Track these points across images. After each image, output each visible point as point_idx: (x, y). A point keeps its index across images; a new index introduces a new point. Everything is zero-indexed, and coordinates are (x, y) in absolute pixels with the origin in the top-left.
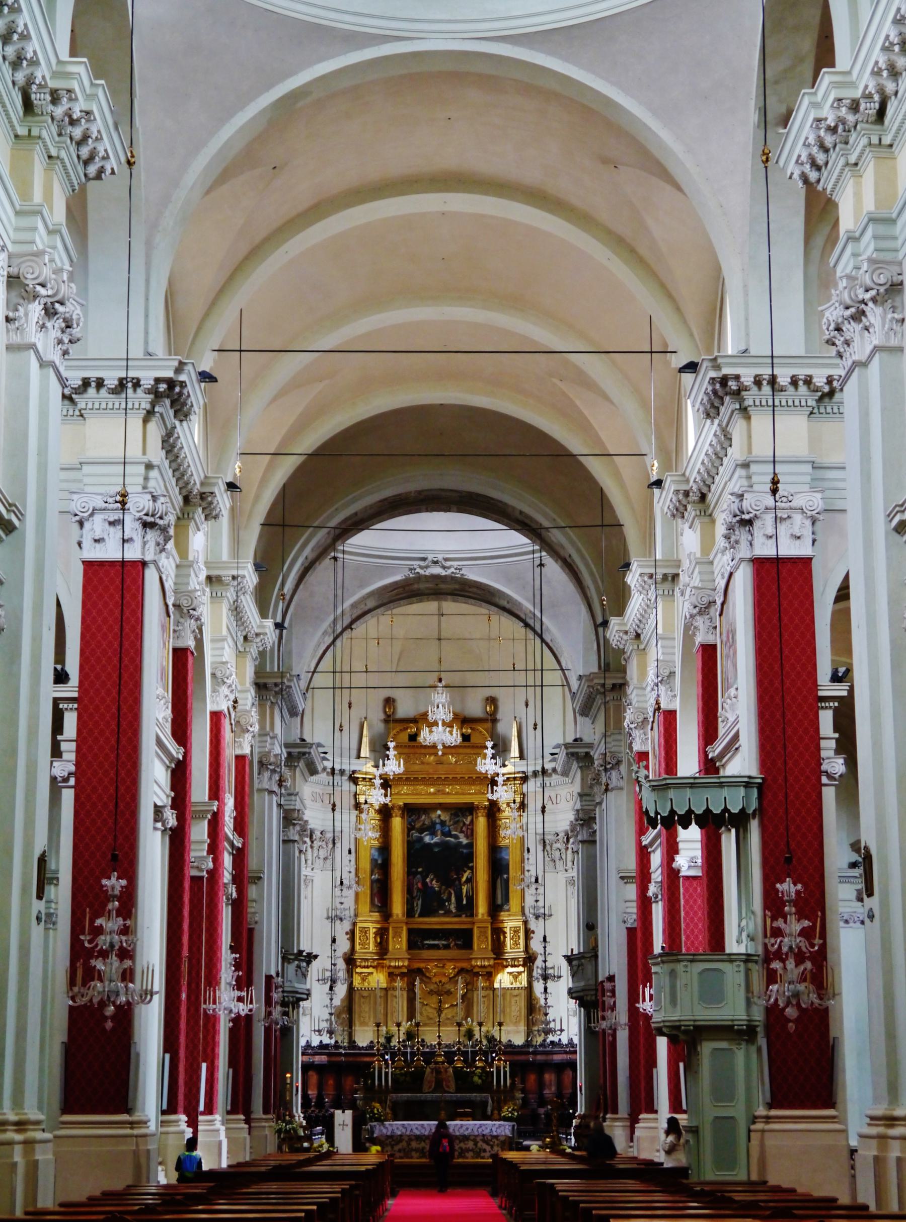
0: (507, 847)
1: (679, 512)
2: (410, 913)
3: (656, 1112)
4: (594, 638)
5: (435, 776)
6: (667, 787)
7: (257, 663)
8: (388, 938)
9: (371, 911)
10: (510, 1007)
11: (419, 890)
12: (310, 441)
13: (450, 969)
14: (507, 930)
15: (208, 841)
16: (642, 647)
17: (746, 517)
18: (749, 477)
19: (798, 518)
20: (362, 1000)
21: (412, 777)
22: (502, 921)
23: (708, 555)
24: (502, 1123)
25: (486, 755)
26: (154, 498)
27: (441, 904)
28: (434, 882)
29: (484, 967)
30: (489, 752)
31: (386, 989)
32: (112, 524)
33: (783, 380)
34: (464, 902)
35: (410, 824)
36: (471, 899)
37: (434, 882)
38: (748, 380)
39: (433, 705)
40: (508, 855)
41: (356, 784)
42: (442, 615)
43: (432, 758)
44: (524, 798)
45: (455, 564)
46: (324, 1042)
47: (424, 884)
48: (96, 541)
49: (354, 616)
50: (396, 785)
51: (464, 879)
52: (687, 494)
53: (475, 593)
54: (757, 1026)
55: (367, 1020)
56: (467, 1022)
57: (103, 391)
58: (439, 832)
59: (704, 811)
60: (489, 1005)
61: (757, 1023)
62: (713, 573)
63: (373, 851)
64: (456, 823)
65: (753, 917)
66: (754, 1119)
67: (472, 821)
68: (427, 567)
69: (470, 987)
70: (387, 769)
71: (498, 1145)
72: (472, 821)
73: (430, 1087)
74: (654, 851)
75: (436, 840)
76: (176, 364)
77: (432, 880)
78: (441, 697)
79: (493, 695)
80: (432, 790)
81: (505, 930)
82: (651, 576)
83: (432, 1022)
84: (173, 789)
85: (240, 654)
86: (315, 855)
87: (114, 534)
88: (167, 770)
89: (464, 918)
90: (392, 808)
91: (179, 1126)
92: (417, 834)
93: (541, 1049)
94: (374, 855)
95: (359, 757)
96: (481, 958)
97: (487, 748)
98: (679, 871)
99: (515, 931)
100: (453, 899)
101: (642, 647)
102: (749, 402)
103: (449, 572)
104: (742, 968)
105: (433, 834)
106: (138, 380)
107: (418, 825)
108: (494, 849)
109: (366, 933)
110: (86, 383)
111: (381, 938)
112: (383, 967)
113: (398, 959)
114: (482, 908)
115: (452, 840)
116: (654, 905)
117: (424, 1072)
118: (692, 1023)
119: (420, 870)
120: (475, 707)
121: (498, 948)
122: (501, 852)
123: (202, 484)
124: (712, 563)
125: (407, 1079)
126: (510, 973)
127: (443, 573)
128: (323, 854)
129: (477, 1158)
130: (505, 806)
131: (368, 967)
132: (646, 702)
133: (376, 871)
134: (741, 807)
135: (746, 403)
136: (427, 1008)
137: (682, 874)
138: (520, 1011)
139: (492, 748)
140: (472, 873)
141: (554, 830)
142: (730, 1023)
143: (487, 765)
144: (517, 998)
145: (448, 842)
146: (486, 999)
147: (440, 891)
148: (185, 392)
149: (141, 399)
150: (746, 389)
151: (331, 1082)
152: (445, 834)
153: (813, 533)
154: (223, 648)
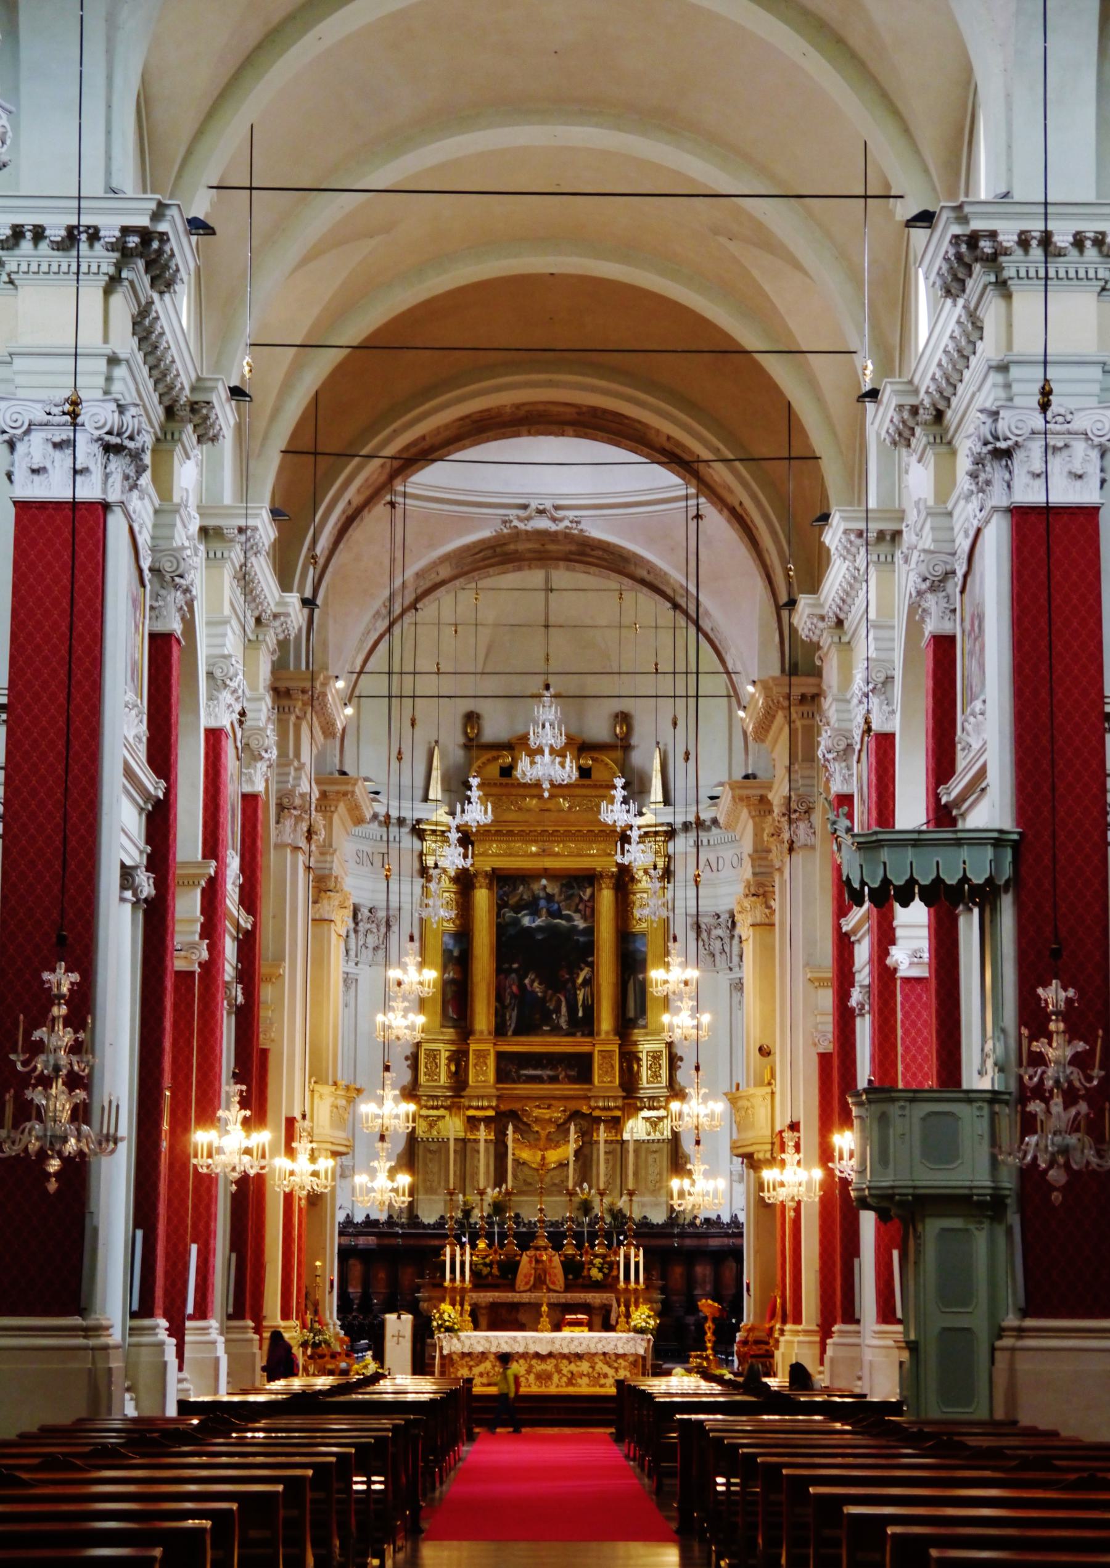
1: (903, 437)
2: (500, 1031)
3: (858, 1322)
4: (776, 626)
5: (539, 829)
6: (878, 845)
7: (275, 658)
8: (467, 1065)
9: (443, 1026)
10: (646, 1168)
11: (513, 996)
12: (355, 331)
14: (643, 1056)
15: (202, 919)
16: (845, 639)
17: (1002, 445)
18: (1008, 386)
19: (1079, 447)
20: (429, 1156)
21: (505, 829)
22: (635, 1043)
23: (945, 502)
24: (632, 1334)
25: (613, 797)
26: (121, 409)
27: (546, 1017)
28: (536, 984)
29: (609, 1109)
30: (619, 794)
32: (58, 446)
33: (1063, 239)
34: (580, 1014)
35: (500, 898)
36: (590, 1010)
37: (536, 984)
38: (1008, 239)
39: (536, 723)
40: (645, 945)
41: (422, 838)
42: (551, 590)
43: (534, 801)
44: (669, 862)
45: (571, 514)
46: (373, 1217)
47: (522, 987)
48: (35, 471)
49: (419, 591)
50: (480, 841)
51: (580, 980)
52: (914, 411)
53: (598, 558)
54: (1007, 1196)
55: (435, 1184)
56: (582, 1189)
57: (44, 246)
58: (544, 911)
59: (933, 880)
61: (1007, 1192)
62: (952, 529)
63: (446, 939)
64: (569, 898)
65: (1002, 1037)
66: (1000, 1332)
67: (592, 896)
68: (529, 518)
69: (586, 1139)
70: (467, 817)
71: (625, 1368)
72: (592, 896)
73: (527, 1283)
74: (859, 941)
75: (539, 922)
76: (153, 205)
77: (532, 982)
78: (548, 712)
79: (626, 710)
80: (534, 849)
81: (640, 1055)
82: (860, 534)
83: (531, 1188)
84: (148, 841)
85: (251, 645)
86: (361, 943)
87: (61, 462)
88: (140, 814)
90: (475, 875)
91: (156, 1334)
92: (512, 914)
93: (691, 1230)
94: (446, 944)
95: (426, 799)
97: (615, 787)
98: (895, 970)
99: (653, 1057)
100: (564, 1010)
101: (845, 639)
102: (1009, 272)
103: (561, 526)
104: (986, 1112)
105: (535, 913)
106: (97, 229)
108: (625, 936)
109: (435, 1057)
110: (18, 233)
111: (457, 1066)
112: (459, 1108)
114: (606, 1022)
115: (563, 922)
116: (858, 1020)
117: (519, 1262)
118: (910, 1191)
119: (515, 966)
120: (599, 729)
121: (629, 1083)
122: (634, 942)
123: (193, 389)
124: (950, 514)
125: (495, 1271)
126: (647, 1119)
127: (553, 527)
128: (372, 940)
129: (593, 1386)
130: (641, 873)
131: (437, 1108)
132: (851, 720)
133: (450, 967)
134: (987, 875)
135: (1006, 274)
136: (525, 1169)
137: (899, 974)
139: (623, 788)
140: (593, 972)
141: (712, 909)
142: (966, 1191)
143: (615, 814)
144: (655, 1156)
145: (556, 926)
146: (610, 1157)
147: (544, 998)
148: (167, 248)
149: (102, 260)
150: (1006, 252)
151: (382, 1275)
152: (552, 914)
153: (1102, 470)
154: (224, 635)
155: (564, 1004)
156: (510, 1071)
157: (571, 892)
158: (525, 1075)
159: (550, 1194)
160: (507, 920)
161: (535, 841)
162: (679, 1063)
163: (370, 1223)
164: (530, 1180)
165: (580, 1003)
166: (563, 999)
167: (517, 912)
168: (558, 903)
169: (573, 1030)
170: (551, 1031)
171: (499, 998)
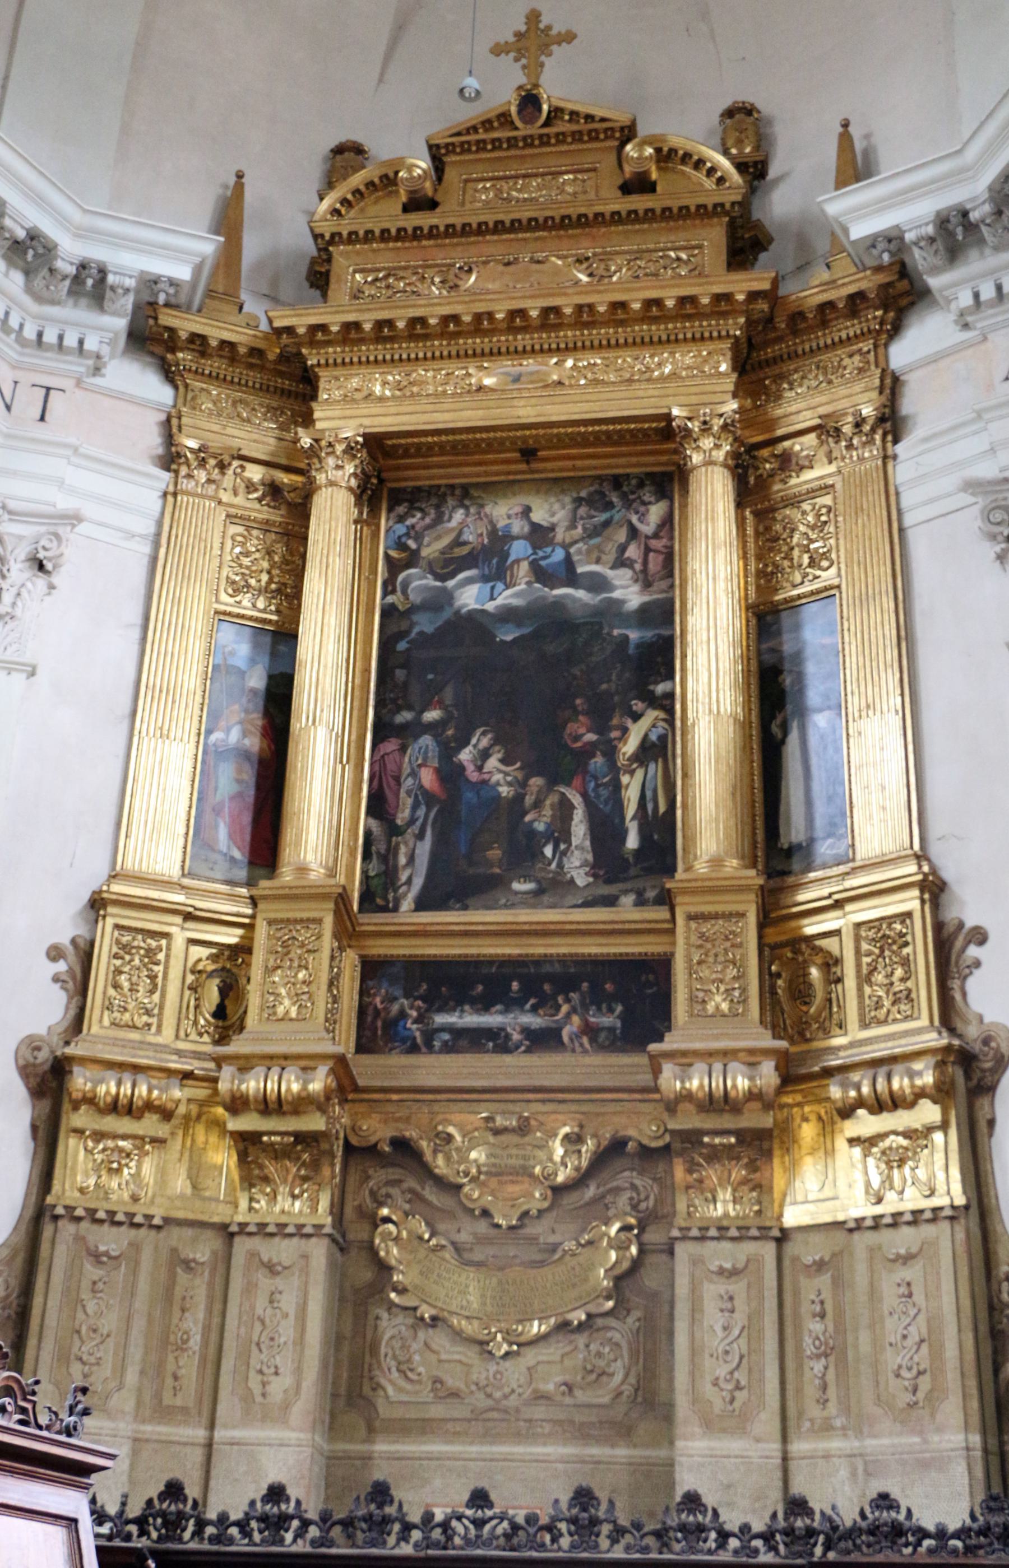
0: (826, 594)
10: (875, 1324)
11: (424, 797)
20: (91, 1271)
31: (228, 1233)
34: (632, 842)
37: (493, 763)
58: (525, 566)
60: (755, 1317)
69: (654, 1236)
72: (667, 522)
75: (506, 597)
77: (485, 755)
80: (488, 381)
81: (830, 944)
83: (459, 1411)
92: (431, 582)
96: (709, 1055)
100: (579, 829)
107: (431, 549)
109: (150, 953)
113: (283, 1060)
115: (581, 594)
119: (432, 715)
122: (797, 627)
126: (866, 1143)
131: (130, 1109)
136: (439, 1339)
138: (931, 1340)
140: (671, 721)
144: (906, 1273)
145: (558, 604)
146: (738, 1287)
147: (519, 798)
152: (541, 574)
155: (579, 815)
156: (403, 1015)
157: (604, 517)
158: (451, 1029)
160: (415, 598)
161: (494, 354)
162: (973, 951)
164: (450, 1382)
165: (631, 809)
166: (577, 800)
167: (443, 578)
168: (566, 547)
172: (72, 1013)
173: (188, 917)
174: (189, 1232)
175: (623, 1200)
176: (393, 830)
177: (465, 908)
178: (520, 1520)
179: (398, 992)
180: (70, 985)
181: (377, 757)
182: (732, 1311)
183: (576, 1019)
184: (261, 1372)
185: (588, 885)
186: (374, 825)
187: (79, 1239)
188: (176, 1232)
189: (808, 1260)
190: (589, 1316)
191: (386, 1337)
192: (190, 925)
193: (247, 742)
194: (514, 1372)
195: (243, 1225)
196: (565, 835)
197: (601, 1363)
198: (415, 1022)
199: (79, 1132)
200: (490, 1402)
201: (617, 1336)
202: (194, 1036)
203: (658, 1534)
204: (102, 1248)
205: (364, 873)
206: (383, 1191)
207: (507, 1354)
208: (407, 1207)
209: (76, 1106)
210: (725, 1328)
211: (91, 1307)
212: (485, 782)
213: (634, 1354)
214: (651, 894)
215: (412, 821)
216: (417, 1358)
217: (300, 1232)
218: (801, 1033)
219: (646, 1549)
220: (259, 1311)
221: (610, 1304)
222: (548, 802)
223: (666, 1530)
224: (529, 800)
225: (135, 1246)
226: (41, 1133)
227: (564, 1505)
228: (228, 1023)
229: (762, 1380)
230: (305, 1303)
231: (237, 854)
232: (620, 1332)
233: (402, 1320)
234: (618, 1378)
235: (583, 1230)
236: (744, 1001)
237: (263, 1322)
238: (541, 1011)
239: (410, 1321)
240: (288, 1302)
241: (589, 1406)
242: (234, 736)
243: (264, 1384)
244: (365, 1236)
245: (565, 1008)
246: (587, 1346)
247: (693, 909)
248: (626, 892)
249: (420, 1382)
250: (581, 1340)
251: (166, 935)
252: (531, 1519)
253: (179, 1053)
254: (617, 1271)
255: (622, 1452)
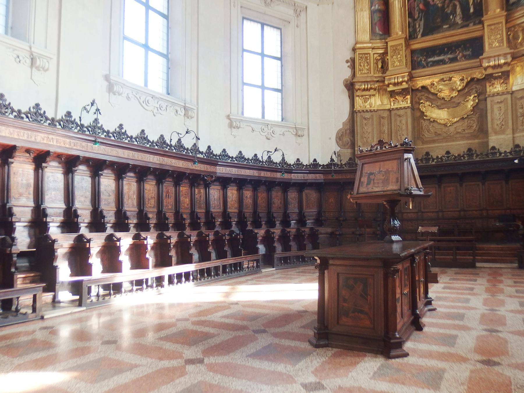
11: (420, 11)
13: (458, 82)
20: (365, 122)
27: (445, 18)
29: (500, 66)
31: (390, 110)
34: (472, 10)
69: (482, 97)
89: (472, 27)
96: (495, 56)
100: (458, 10)
136: (435, 124)
146: (502, 105)
147: (443, 6)
151: (332, 200)
155: (458, 7)
156: (421, 60)
159: (456, 140)
163: (315, 164)
164: (438, 132)
165: (471, 3)
166: (457, 3)
169: (465, 23)
170: (449, 27)
171: (411, 15)
172: (352, 73)
173: (373, 48)
174: (382, 112)
175: (474, 91)
176: (414, 20)
177: (433, 34)
178: (457, 155)
179: (419, 55)
180: (351, 67)
181: (409, 4)
182: (501, 110)
183: (461, 54)
184: (400, 135)
185: (461, 23)
186: (410, 20)
187: (361, 116)
188: (379, 112)
189: (519, 97)
190: (468, 116)
191: (424, 126)
192: (373, 50)
193: (379, 7)
194: (452, 129)
195: (393, 109)
196: (455, 13)
197: (471, 124)
198: (424, 61)
199: (358, 96)
200: (447, 135)
201: (474, 119)
202: (377, 73)
203: (486, 155)
204: (366, 117)
205: (409, 31)
206: (421, 97)
207: (450, 125)
208: (426, 100)
209: (357, 91)
210: (499, 114)
211: (366, 128)
212: (435, 4)
213: (478, 122)
214: (477, 22)
215: (419, 17)
216: (431, 129)
217: (405, 108)
218: (516, 47)
219: (484, 158)
220: (398, 124)
221: (472, 112)
222: (451, 5)
223: (488, 154)
224: (446, 6)
225: (372, 116)
226: (351, 97)
227: (466, 151)
228: (384, 69)
229: (508, 123)
230: (407, 122)
231: (381, 33)
232: (475, 118)
233: (427, 122)
234: (475, 127)
235: (466, 98)
236: (503, 42)
237: (399, 126)
238: (452, 54)
239: (429, 122)
240: (404, 122)
241: (469, 133)
242: (377, 6)
243: (401, 138)
244: (418, 107)
245: (458, 52)
246: (468, 121)
247: (489, 23)
248: (471, 23)
249: (432, 133)
250: (466, 120)
251: (369, 54)
252: (459, 155)
253: (375, 77)
254: (473, 106)
255: (476, 141)
